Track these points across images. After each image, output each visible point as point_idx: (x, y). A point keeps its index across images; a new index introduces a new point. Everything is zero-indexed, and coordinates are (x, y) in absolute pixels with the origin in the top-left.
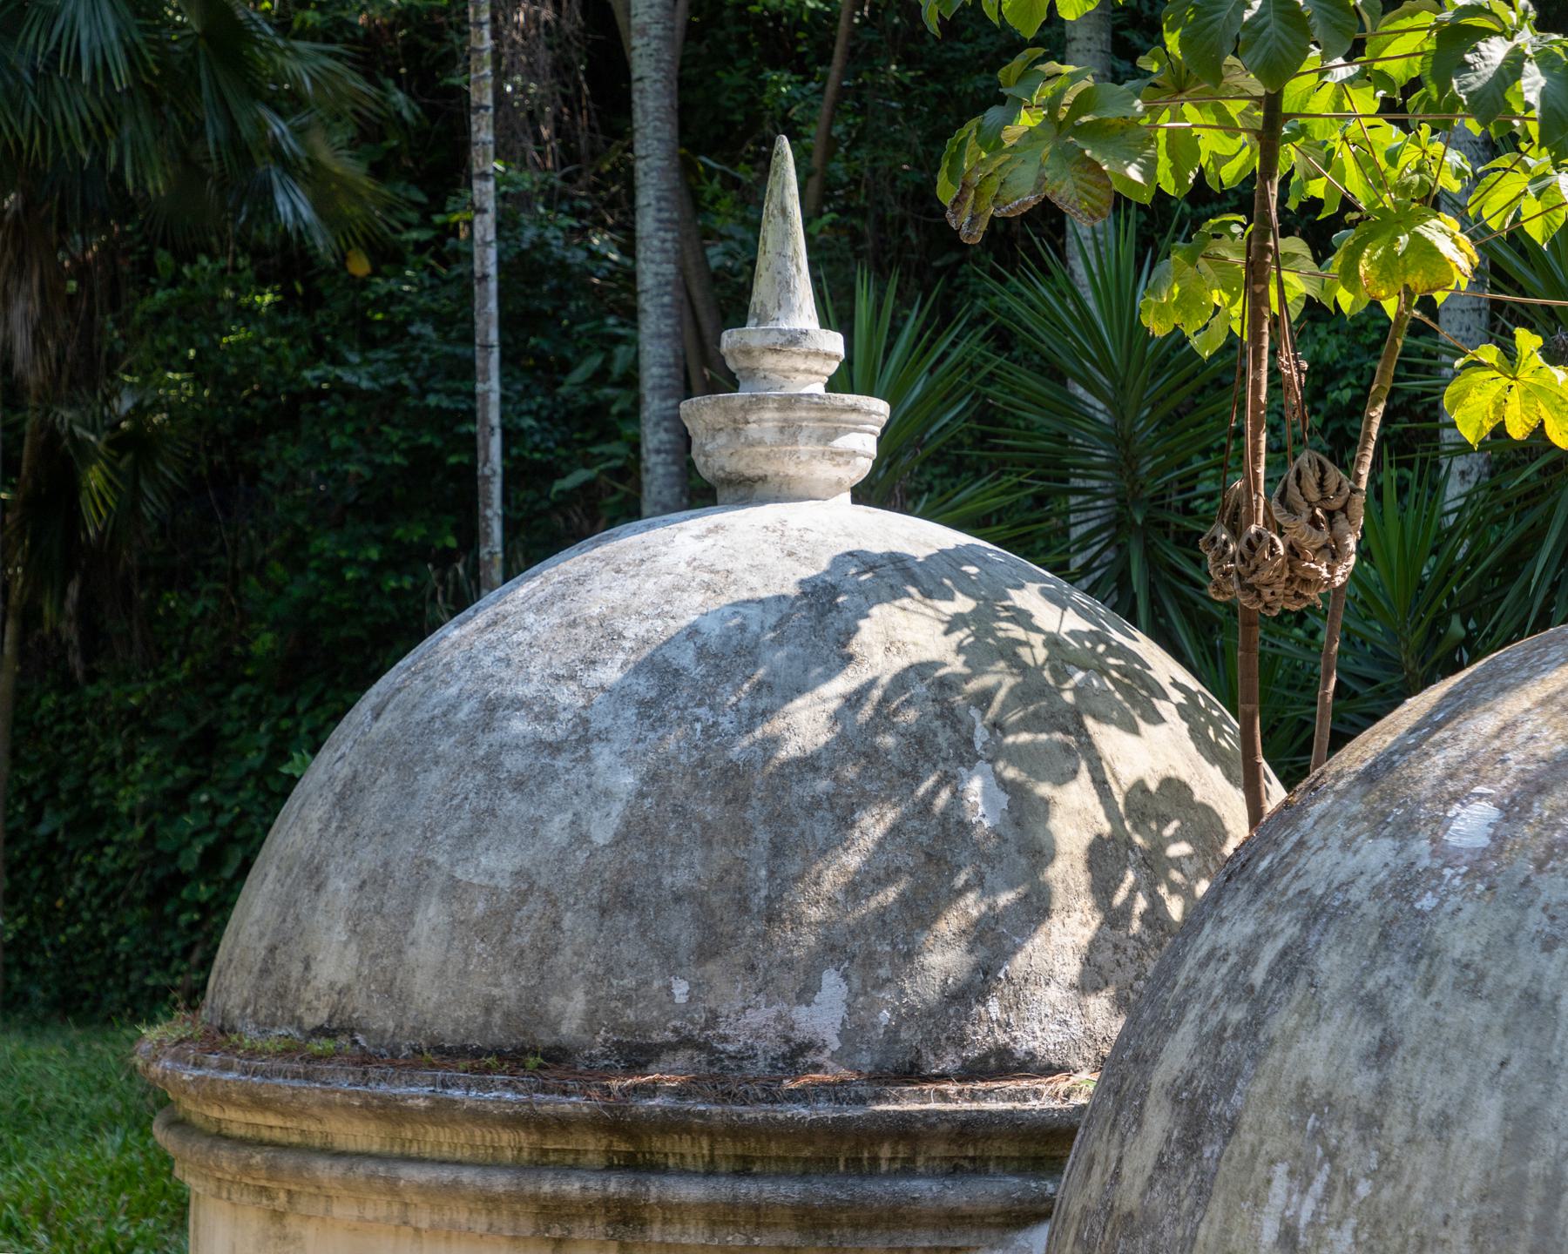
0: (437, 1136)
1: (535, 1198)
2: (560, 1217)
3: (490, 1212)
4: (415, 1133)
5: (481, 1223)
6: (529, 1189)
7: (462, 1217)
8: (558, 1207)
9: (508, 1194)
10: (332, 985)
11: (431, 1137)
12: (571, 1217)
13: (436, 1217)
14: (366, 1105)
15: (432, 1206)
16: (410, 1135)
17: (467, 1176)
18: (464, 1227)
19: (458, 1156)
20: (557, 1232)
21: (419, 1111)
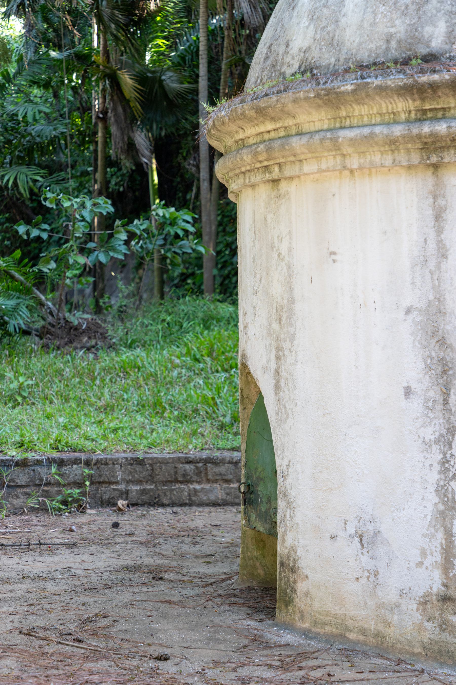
0: (360, 111)
1: (419, 136)
2: (435, 150)
3: (393, 151)
4: (347, 111)
5: (388, 159)
6: (415, 131)
7: (377, 158)
8: (434, 142)
9: (403, 137)
10: (300, 50)
11: (357, 113)
12: (442, 148)
13: (362, 161)
14: (318, 96)
15: (359, 153)
16: (344, 114)
17: (377, 130)
18: (379, 164)
19: (373, 122)
20: (434, 159)
21: (348, 93)
